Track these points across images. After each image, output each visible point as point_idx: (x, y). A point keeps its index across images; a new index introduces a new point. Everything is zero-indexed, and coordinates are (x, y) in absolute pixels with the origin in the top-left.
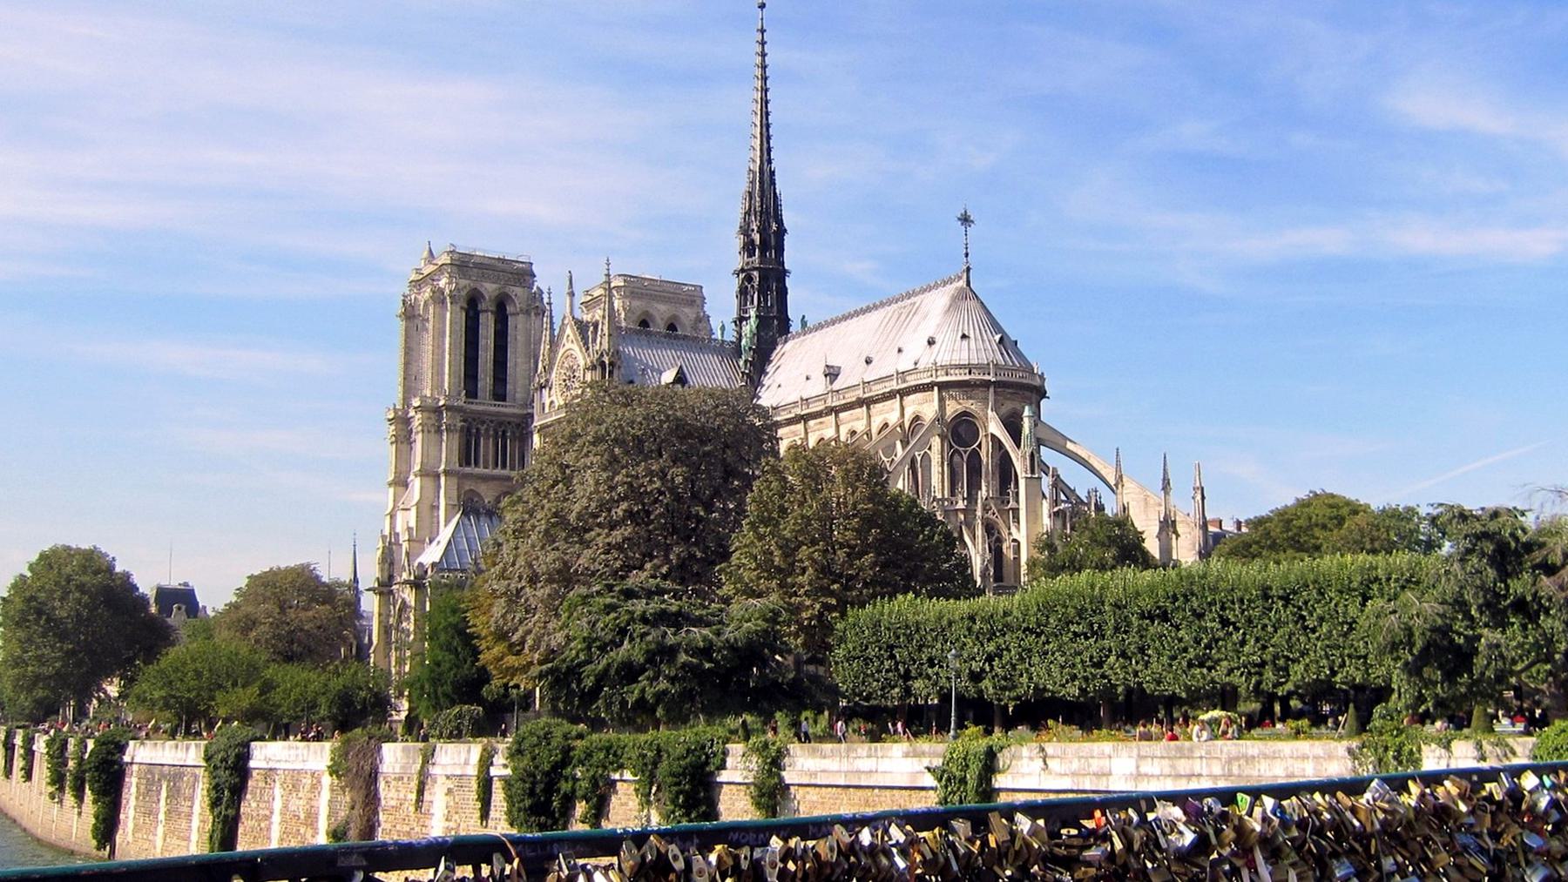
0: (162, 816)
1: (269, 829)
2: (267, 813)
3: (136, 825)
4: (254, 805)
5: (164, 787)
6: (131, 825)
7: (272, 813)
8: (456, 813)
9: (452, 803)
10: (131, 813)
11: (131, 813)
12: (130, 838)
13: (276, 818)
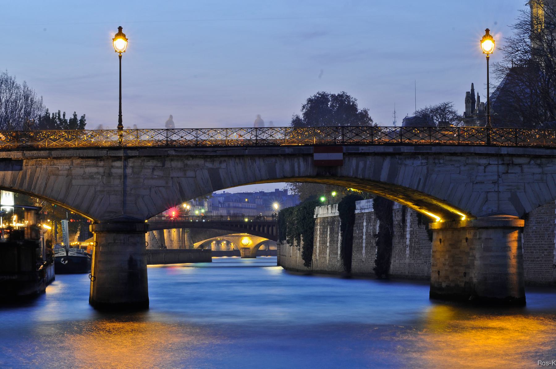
0: (328, 244)
1: (362, 242)
2: (361, 235)
3: (320, 250)
4: (357, 232)
5: (329, 229)
6: (318, 251)
7: (363, 235)
8: (413, 224)
9: (412, 220)
10: (318, 244)
11: (318, 244)
12: (318, 258)
13: (364, 237)
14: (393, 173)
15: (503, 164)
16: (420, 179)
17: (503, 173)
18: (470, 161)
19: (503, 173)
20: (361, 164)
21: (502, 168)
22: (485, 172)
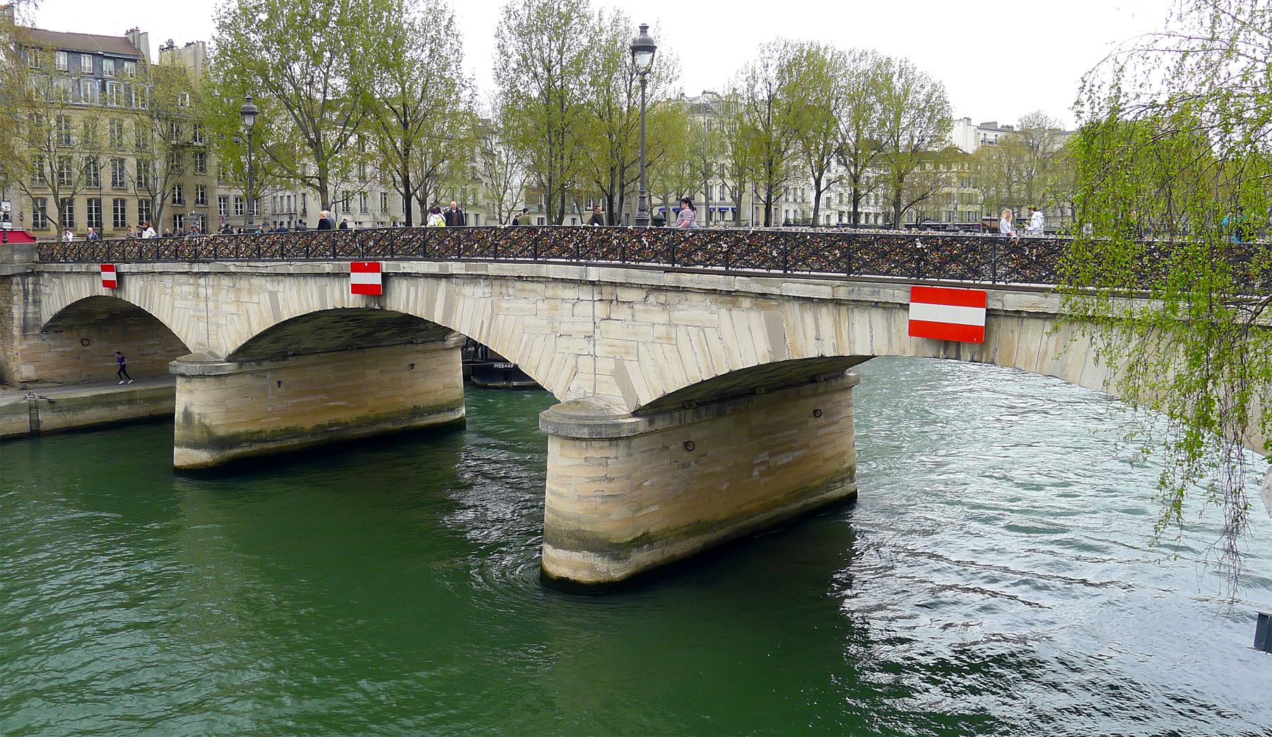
14: (449, 309)
15: (601, 300)
16: (483, 323)
17: (603, 319)
18: (550, 293)
19: (603, 319)
20: (412, 290)
21: (601, 310)
22: (573, 316)
